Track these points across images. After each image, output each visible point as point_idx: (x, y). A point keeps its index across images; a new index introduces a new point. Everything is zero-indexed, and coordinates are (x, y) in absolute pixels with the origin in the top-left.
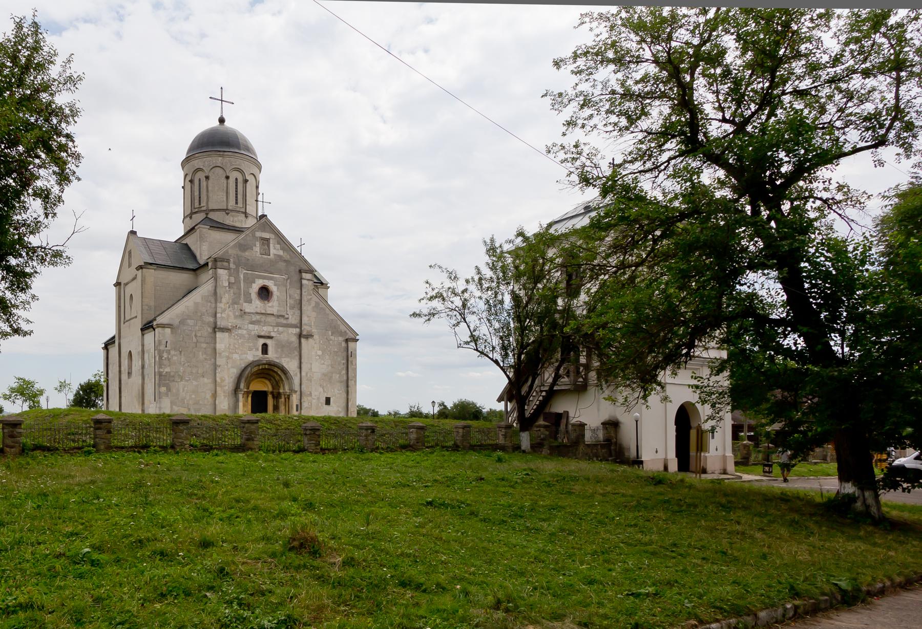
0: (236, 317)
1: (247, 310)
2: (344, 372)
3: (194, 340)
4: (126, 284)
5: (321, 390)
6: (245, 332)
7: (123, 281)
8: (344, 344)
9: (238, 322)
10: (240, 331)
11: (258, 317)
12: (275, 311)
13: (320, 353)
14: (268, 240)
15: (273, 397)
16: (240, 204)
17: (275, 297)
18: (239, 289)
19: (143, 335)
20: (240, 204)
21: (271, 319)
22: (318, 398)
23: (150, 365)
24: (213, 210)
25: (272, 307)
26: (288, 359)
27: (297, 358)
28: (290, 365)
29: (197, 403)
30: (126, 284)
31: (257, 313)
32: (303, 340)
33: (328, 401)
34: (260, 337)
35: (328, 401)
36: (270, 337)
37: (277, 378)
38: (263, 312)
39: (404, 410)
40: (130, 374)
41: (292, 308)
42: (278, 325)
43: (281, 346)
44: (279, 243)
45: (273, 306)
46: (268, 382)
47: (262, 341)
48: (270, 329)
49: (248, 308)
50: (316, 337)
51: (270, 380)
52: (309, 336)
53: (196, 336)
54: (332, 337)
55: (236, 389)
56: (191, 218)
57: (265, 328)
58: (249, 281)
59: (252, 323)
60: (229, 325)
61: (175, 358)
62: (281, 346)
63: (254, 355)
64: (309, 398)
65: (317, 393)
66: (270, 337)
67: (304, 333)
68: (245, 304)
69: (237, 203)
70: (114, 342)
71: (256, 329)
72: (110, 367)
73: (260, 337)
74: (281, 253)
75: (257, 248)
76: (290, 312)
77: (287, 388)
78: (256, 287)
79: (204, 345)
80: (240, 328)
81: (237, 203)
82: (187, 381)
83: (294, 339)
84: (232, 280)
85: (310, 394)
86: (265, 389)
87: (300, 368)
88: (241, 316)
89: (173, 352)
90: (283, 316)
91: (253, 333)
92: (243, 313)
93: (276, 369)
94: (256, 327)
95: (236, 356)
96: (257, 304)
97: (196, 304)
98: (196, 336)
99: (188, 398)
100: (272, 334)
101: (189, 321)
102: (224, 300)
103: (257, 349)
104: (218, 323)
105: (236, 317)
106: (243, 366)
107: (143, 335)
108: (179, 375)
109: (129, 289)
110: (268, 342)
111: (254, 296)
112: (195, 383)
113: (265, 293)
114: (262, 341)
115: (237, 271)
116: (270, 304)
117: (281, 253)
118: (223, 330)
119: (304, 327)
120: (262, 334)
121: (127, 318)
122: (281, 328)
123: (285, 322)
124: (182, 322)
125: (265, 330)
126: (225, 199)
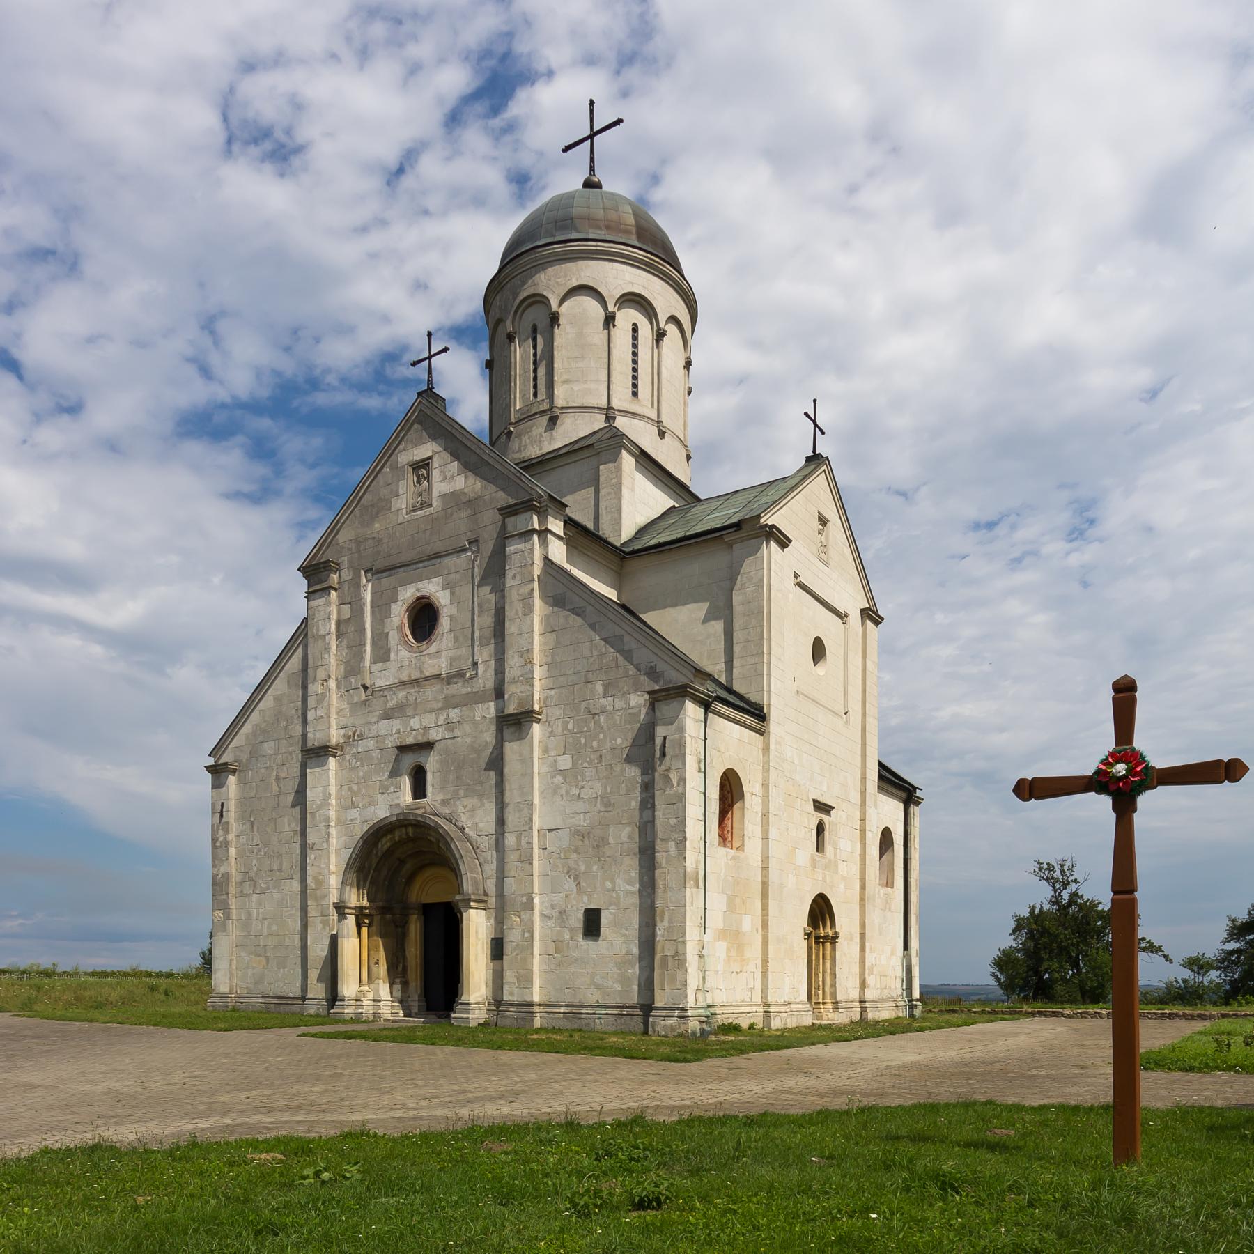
1: (380, 683)
5: (570, 885)
6: (371, 744)
10: (361, 746)
11: (401, 695)
13: (565, 762)
16: (542, 395)
17: (444, 623)
20: (542, 395)
21: (431, 693)
31: (401, 684)
33: (592, 924)
35: (592, 924)
38: (416, 675)
39: (1139, 911)
42: (449, 703)
45: (442, 652)
47: (409, 760)
48: (429, 719)
49: (382, 677)
54: (606, 702)
59: (387, 715)
66: (428, 746)
71: (393, 732)
73: (403, 749)
78: (399, 614)
80: (361, 737)
81: (535, 395)
85: (529, 906)
90: (460, 675)
91: (389, 743)
94: (396, 724)
99: (265, 931)
100: (434, 735)
101: (265, 745)
104: (310, 735)
108: (251, 880)
113: (424, 619)
116: (433, 648)
120: (410, 740)
122: (454, 714)
125: (416, 727)
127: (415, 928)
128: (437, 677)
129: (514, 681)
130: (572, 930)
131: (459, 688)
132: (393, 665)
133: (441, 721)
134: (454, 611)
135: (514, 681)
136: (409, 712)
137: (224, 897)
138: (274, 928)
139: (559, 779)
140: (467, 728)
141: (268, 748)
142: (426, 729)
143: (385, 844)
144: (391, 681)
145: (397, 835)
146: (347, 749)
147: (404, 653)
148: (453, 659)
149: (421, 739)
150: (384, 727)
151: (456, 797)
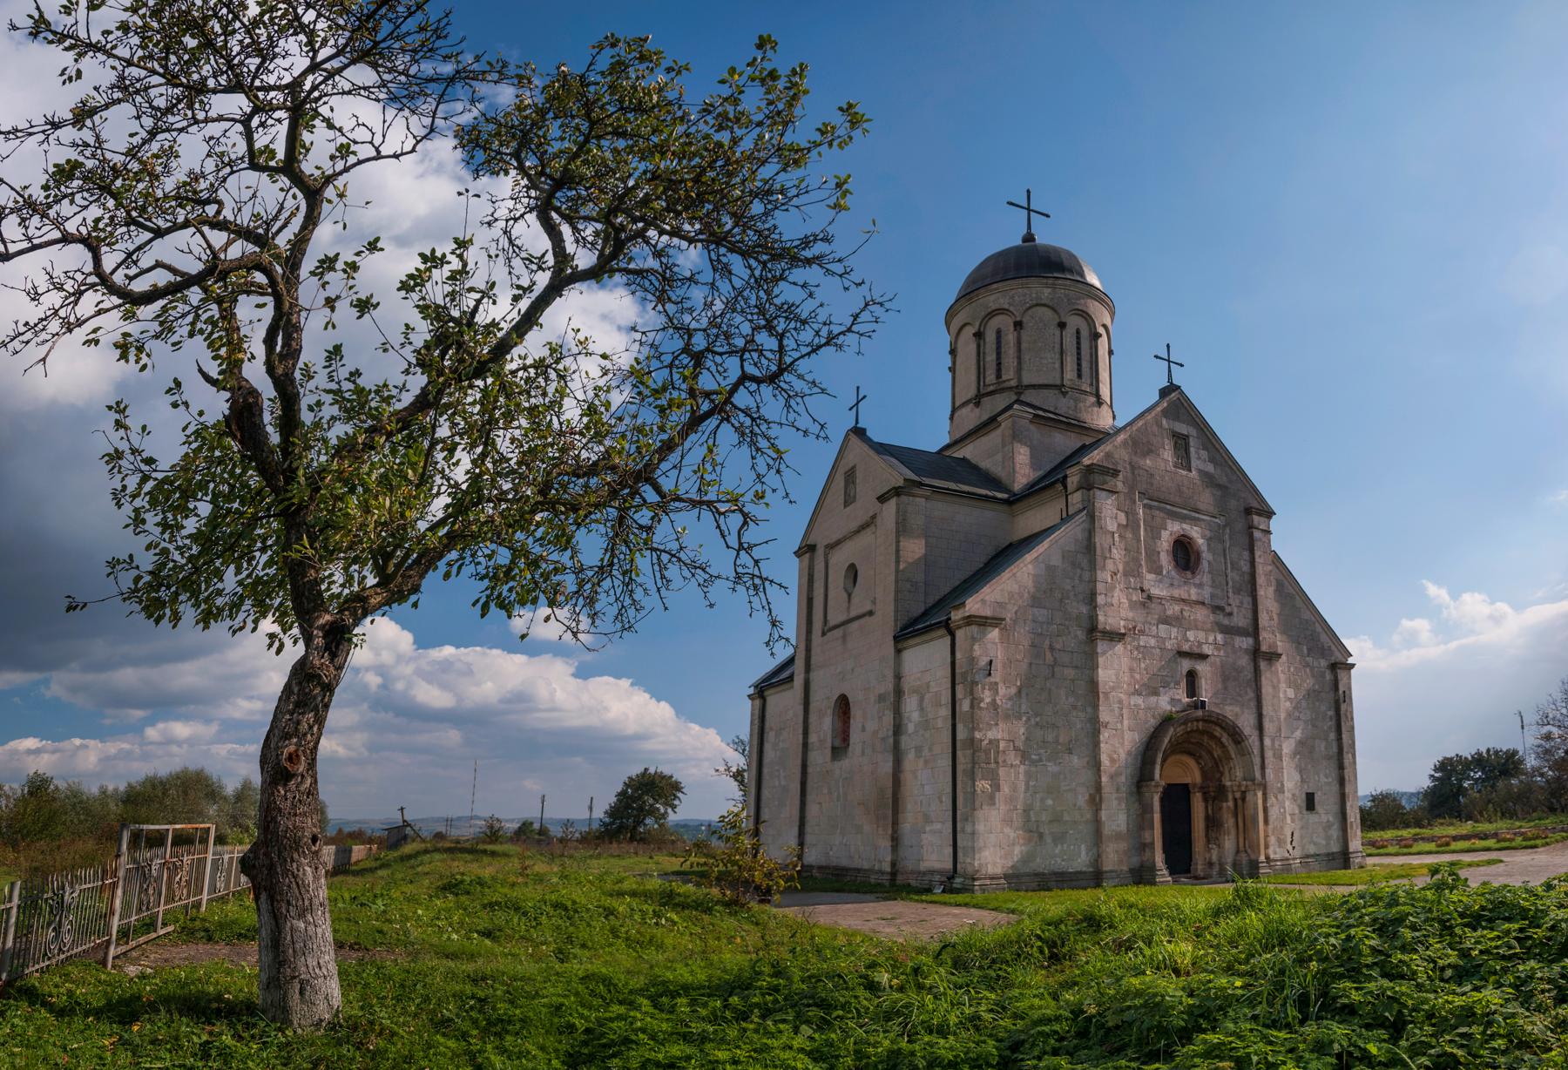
2: (1332, 736)
4: (831, 547)
6: (1152, 642)
7: (821, 540)
8: (1328, 676)
10: (1143, 641)
15: (1206, 800)
17: (1205, 565)
19: (898, 651)
23: (925, 724)
24: (1033, 387)
27: (1253, 704)
30: (831, 547)
32: (1263, 665)
36: (1203, 657)
37: (1217, 752)
40: (840, 749)
41: (1237, 591)
46: (1191, 762)
47: (1186, 665)
48: (1201, 635)
50: (1284, 657)
51: (1197, 759)
52: (1273, 656)
53: (1052, 648)
55: (1142, 777)
56: (977, 404)
57: (1191, 635)
59: (1165, 620)
60: (1121, 626)
66: (1203, 657)
67: (1264, 648)
69: (1080, 376)
70: (791, 678)
72: (770, 736)
73: (1182, 654)
74: (1210, 468)
75: (1168, 454)
76: (1234, 600)
77: (1239, 774)
79: (1070, 673)
80: (1142, 632)
81: (1080, 376)
83: (1244, 661)
86: (1188, 780)
89: (1002, 690)
91: (1168, 645)
93: (1218, 732)
98: (1052, 648)
100: (1207, 650)
102: (1110, 565)
105: (1133, 605)
106: (1153, 722)
107: (898, 651)
109: (840, 559)
111: (1165, 560)
118: (1115, 636)
119: (1263, 635)
121: (832, 622)
123: (1226, 622)
126: (1057, 365)
133: (1211, 639)
134: (1210, 557)
137: (993, 766)
138: (1050, 802)
142: (1200, 644)
146: (1128, 639)
149: (1196, 650)
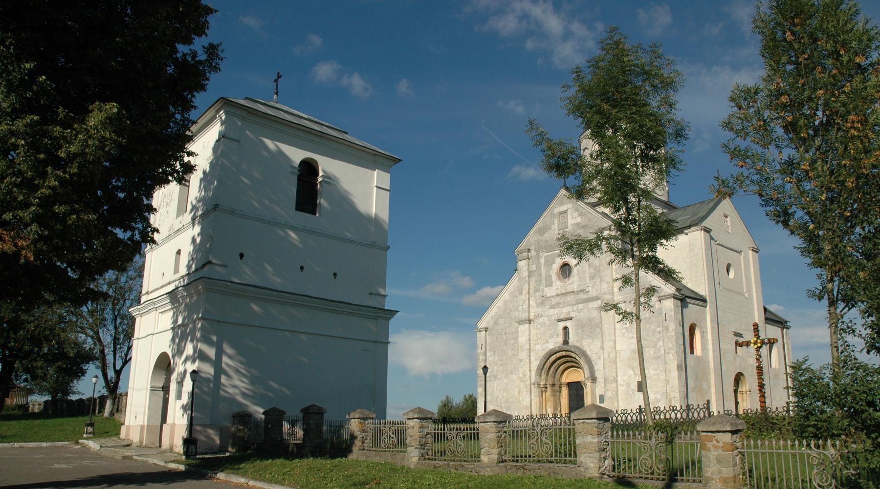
0: (538, 306)
1: (548, 295)
3: (505, 338)
6: (546, 319)
9: (539, 310)
10: (541, 320)
12: (575, 287)
14: (565, 212)
18: (540, 275)
21: (570, 298)
22: (628, 385)
25: (572, 283)
26: (589, 341)
27: (599, 336)
28: (591, 347)
29: (507, 401)
31: (558, 295)
34: (559, 321)
36: (571, 319)
38: (564, 291)
42: (578, 302)
43: (581, 325)
44: (576, 210)
47: (562, 325)
48: (569, 309)
49: (550, 292)
57: (564, 310)
58: (549, 263)
59: (552, 307)
61: (491, 359)
62: (581, 325)
63: (555, 342)
64: (614, 385)
65: (626, 378)
66: (571, 319)
68: (546, 289)
71: (555, 313)
79: (512, 341)
82: (500, 379)
84: (534, 267)
87: (602, 348)
88: (542, 303)
89: (488, 354)
90: (582, 291)
92: (544, 300)
94: (557, 310)
95: (538, 347)
96: (558, 285)
97: (505, 302)
100: (572, 315)
103: (558, 335)
105: (538, 306)
110: (568, 324)
111: (554, 277)
112: (506, 381)
114: (562, 325)
115: (538, 257)
116: (570, 281)
117: (579, 220)
120: (562, 317)
122: (580, 306)
123: (585, 296)
124: (496, 323)
125: (564, 312)
127: (565, 392)
128: (573, 292)
129: (605, 293)
130: (632, 390)
131: (583, 296)
132: (554, 288)
135: (605, 293)
136: (561, 306)
139: (624, 331)
140: (586, 311)
141: (501, 321)
143: (553, 358)
144: (554, 294)
145: (558, 355)
147: (558, 283)
148: (579, 286)
149: (567, 316)
150: (551, 312)
151: (582, 339)
